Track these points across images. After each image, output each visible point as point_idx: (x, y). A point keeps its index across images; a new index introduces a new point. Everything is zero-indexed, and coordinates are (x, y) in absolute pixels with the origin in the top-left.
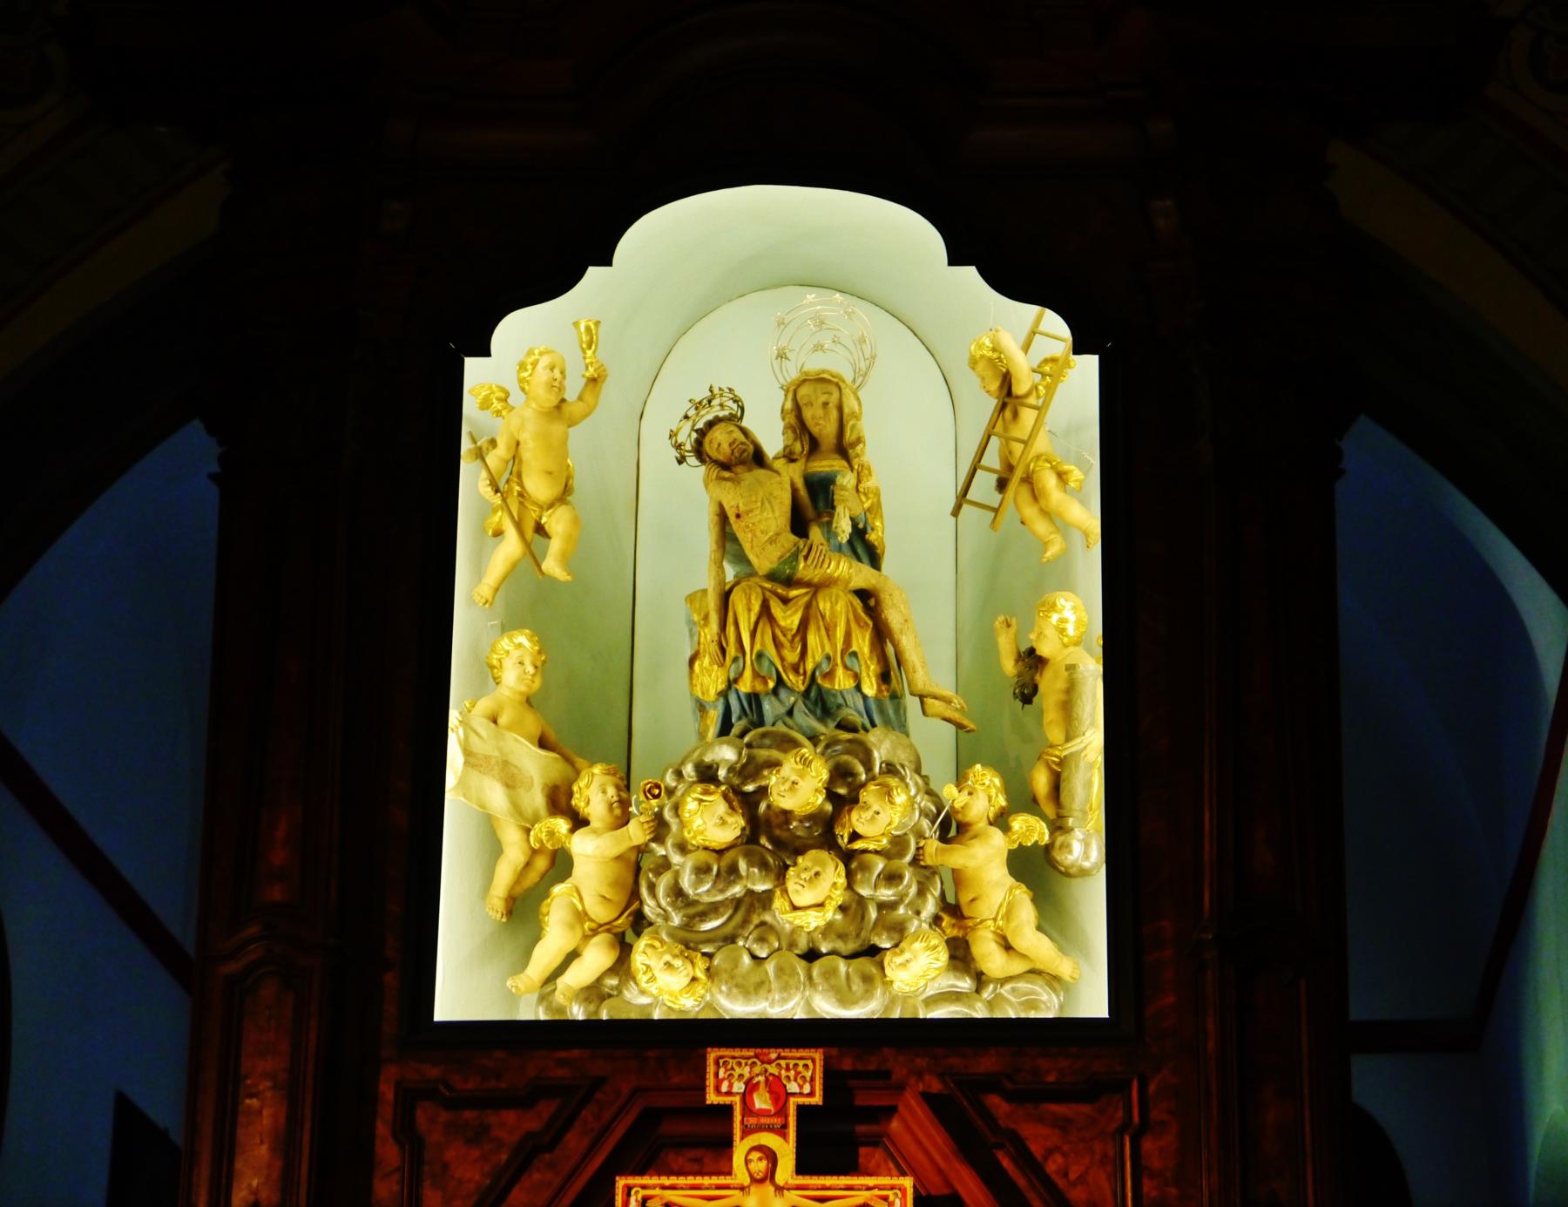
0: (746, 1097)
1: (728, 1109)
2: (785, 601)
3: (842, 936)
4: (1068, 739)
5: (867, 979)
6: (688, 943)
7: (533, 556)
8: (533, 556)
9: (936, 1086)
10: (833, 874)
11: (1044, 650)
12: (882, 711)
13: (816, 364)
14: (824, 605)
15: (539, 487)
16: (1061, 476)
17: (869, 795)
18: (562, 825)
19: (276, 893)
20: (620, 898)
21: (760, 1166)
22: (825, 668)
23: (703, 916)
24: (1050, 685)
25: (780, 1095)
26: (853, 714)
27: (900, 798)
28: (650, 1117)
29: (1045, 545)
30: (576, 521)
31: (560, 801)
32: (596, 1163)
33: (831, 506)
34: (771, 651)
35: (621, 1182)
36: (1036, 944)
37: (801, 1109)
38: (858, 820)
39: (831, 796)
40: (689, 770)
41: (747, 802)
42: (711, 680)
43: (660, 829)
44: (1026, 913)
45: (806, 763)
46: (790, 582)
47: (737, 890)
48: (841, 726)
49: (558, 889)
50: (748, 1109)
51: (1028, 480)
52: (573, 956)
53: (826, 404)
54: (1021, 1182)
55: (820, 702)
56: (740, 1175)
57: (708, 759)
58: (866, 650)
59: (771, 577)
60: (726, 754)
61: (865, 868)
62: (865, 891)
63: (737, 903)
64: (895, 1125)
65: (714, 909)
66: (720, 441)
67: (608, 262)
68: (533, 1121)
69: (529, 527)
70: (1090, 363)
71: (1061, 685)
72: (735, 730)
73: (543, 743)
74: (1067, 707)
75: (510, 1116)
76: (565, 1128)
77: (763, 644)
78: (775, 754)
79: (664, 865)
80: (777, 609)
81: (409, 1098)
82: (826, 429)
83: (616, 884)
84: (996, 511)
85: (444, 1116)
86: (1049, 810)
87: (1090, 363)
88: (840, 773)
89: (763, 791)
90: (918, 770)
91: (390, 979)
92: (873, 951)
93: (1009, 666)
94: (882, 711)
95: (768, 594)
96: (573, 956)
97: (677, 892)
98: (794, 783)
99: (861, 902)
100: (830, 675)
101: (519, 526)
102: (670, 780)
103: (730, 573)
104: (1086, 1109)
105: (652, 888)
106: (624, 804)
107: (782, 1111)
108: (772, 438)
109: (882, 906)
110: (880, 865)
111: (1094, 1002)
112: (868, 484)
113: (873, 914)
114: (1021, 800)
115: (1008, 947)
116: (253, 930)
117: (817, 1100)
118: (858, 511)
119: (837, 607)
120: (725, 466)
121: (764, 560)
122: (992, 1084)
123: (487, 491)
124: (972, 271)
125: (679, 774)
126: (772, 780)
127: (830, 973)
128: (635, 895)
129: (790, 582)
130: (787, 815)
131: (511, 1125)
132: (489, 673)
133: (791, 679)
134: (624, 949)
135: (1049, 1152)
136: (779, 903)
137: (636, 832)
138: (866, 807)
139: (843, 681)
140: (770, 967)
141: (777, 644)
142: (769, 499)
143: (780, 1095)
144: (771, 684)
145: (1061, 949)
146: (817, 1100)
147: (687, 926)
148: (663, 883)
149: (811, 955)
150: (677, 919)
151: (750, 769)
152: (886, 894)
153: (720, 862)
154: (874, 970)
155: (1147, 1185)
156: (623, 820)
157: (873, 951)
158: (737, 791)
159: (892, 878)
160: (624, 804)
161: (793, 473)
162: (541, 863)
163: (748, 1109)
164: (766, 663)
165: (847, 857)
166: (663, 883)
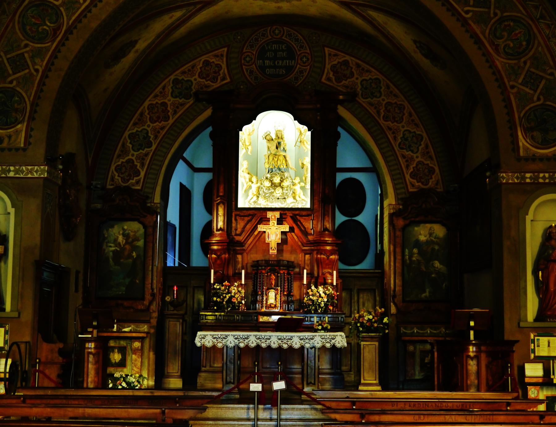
0: (271, 217)
1: (269, 218)
2: (275, 157)
3: (281, 197)
4: (307, 174)
5: (284, 202)
6: (265, 197)
7: (247, 152)
8: (247, 152)
9: (291, 215)
10: (281, 190)
11: (304, 163)
12: (286, 169)
13: (279, 129)
14: (280, 158)
15: (247, 144)
16: (307, 143)
17: (284, 181)
18: (251, 183)
19: (221, 194)
20: (257, 191)
21: (273, 224)
23: (266, 194)
24: (305, 168)
25: (275, 217)
26: (283, 170)
27: (288, 181)
28: (261, 218)
29: (305, 150)
30: (252, 147)
31: (250, 180)
32: (256, 223)
33: (280, 145)
34: (274, 163)
35: (258, 226)
36: (303, 197)
37: (277, 218)
38: (283, 184)
39: (280, 180)
40: (265, 177)
41: (271, 181)
42: (267, 166)
43: (261, 184)
44: (302, 193)
45: (278, 177)
46: (276, 155)
47: (270, 191)
48: (282, 172)
49: (250, 190)
50: (272, 218)
51: (303, 142)
52: (252, 198)
54: (300, 225)
55: (280, 169)
56: (271, 225)
57: (267, 176)
59: (274, 154)
60: (269, 176)
61: (284, 189)
62: (284, 191)
63: (270, 193)
64: (287, 219)
65: (268, 193)
66: (268, 138)
67: (255, 120)
68: (249, 218)
69: (246, 148)
70: (310, 132)
71: (306, 168)
72: (270, 172)
73: (248, 174)
74: (307, 170)
75: (246, 218)
76: (252, 219)
78: (274, 176)
79: (262, 188)
80: (274, 158)
81: (236, 215)
82: (280, 136)
83: (257, 190)
84: (299, 147)
85: (240, 218)
86: (305, 182)
87: (310, 132)
88: (281, 178)
89: (273, 180)
90: (290, 177)
91: (233, 203)
92: (285, 198)
93: (301, 165)
94: (286, 169)
96: (252, 198)
97: (264, 192)
99: (284, 193)
100: (280, 166)
101: (245, 148)
102: (263, 178)
103: (269, 152)
104: (307, 217)
105: (261, 190)
106: (258, 181)
107: (275, 218)
108: (274, 137)
109: (286, 193)
110: (286, 188)
111: (308, 206)
112: (285, 142)
113: (285, 194)
114: (301, 181)
115: (300, 197)
116: (219, 198)
117: (279, 217)
118: (284, 146)
119: (281, 158)
120: (268, 140)
121: (273, 152)
122: (297, 215)
123: (242, 145)
124: (296, 121)
125: (264, 178)
126: (274, 179)
127: (280, 201)
128: (259, 191)
129: (276, 155)
130: (276, 183)
131: (247, 219)
132: (242, 165)
133: (276, 166)
134: (258, 197)
135: (303, 222)
136: (275, 193)
137: (259, 184)
139: (282, 167)
140: (274, 200)
142: (274, 145)
143: (275, 217)
145: (306, 197)
146: (279, 217)
147: (265, 195)
148: (262, 190)
149: (278, 199)
150: (263, 194)
151: (271, 177)
152: (286, 192)
153: (268, 189)
154: (285, 201)
155: (313, 225)
156: (257, 183)
157: (285, 198)
158: (270, 180)
159: (287, 190)
160: (258, 181)
161: (276, 142)
162: (248, 187)
163: (272, 218)
165: (282, 188)
166: (262, 190)
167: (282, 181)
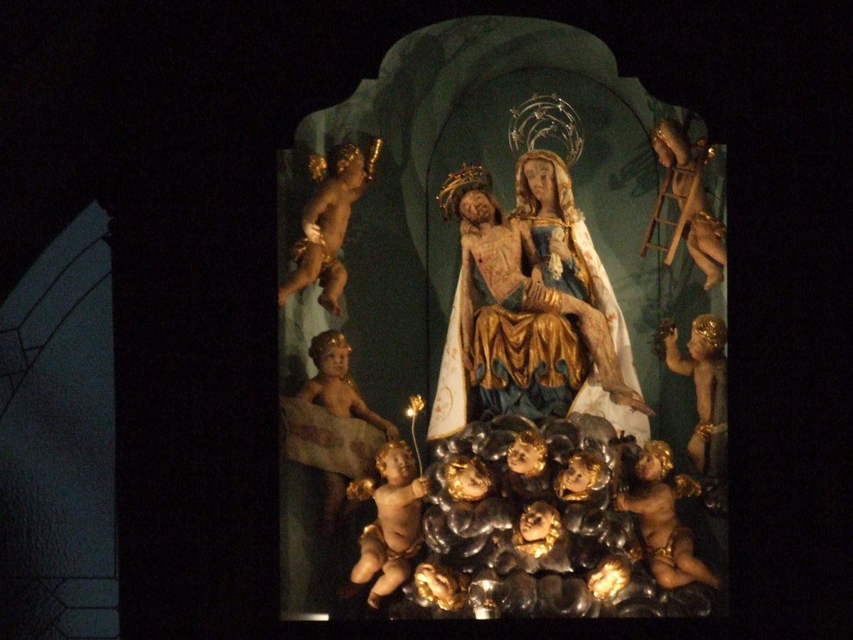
10: (550, 520)
22: (542, 372)
38: (567, 482)
53: (543, 178)
58: (574, 358)
59: (505, 305)
77: (497, 355)
80: (508, 329)
95: (502, 319)
98: (523, 455)
100: (546, 377)
133: (518, 378)
138: (572, 472)
141: (508, 356)
144: (505, 384)
153: (474, 511)
164: (500, 369)
167: (554, 470)
